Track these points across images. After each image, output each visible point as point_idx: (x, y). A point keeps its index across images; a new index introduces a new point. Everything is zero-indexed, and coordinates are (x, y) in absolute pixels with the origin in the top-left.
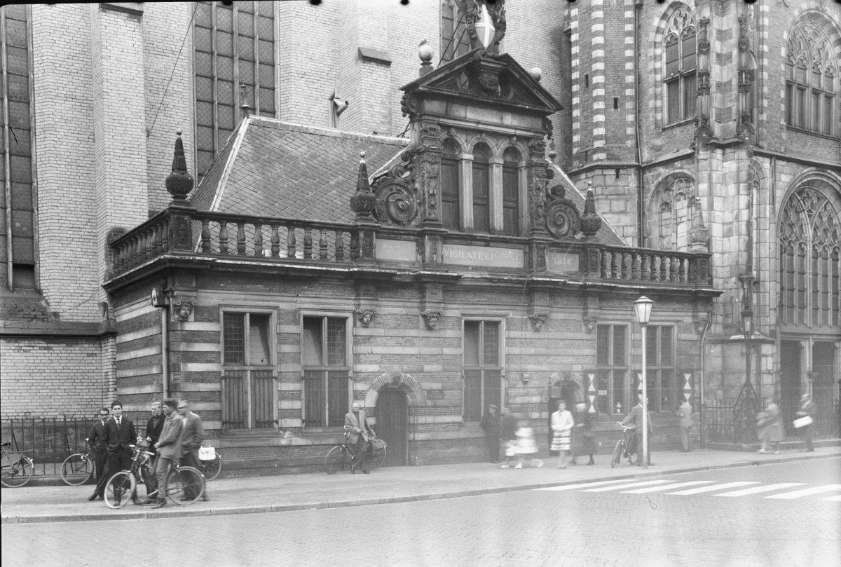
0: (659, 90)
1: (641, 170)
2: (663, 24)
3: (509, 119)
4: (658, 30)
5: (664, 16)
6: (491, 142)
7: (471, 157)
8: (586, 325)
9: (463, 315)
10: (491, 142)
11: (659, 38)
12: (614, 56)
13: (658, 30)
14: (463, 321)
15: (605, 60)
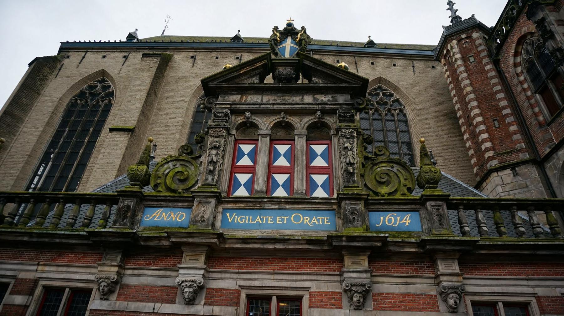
0: (533, 101)
1: (539, 163)
2: (519, 60)
3: (308, 99)
4: (516, 65)
5: (516, 54)
6: (294, 120)
7: (268, 132)
8: (445, 301)
9: (242, 287)
10: (294, 120)
11: (519, 69)
12: (484, 95)
13: (516, 65)
14: (243, 296)
15: (477, 99)
